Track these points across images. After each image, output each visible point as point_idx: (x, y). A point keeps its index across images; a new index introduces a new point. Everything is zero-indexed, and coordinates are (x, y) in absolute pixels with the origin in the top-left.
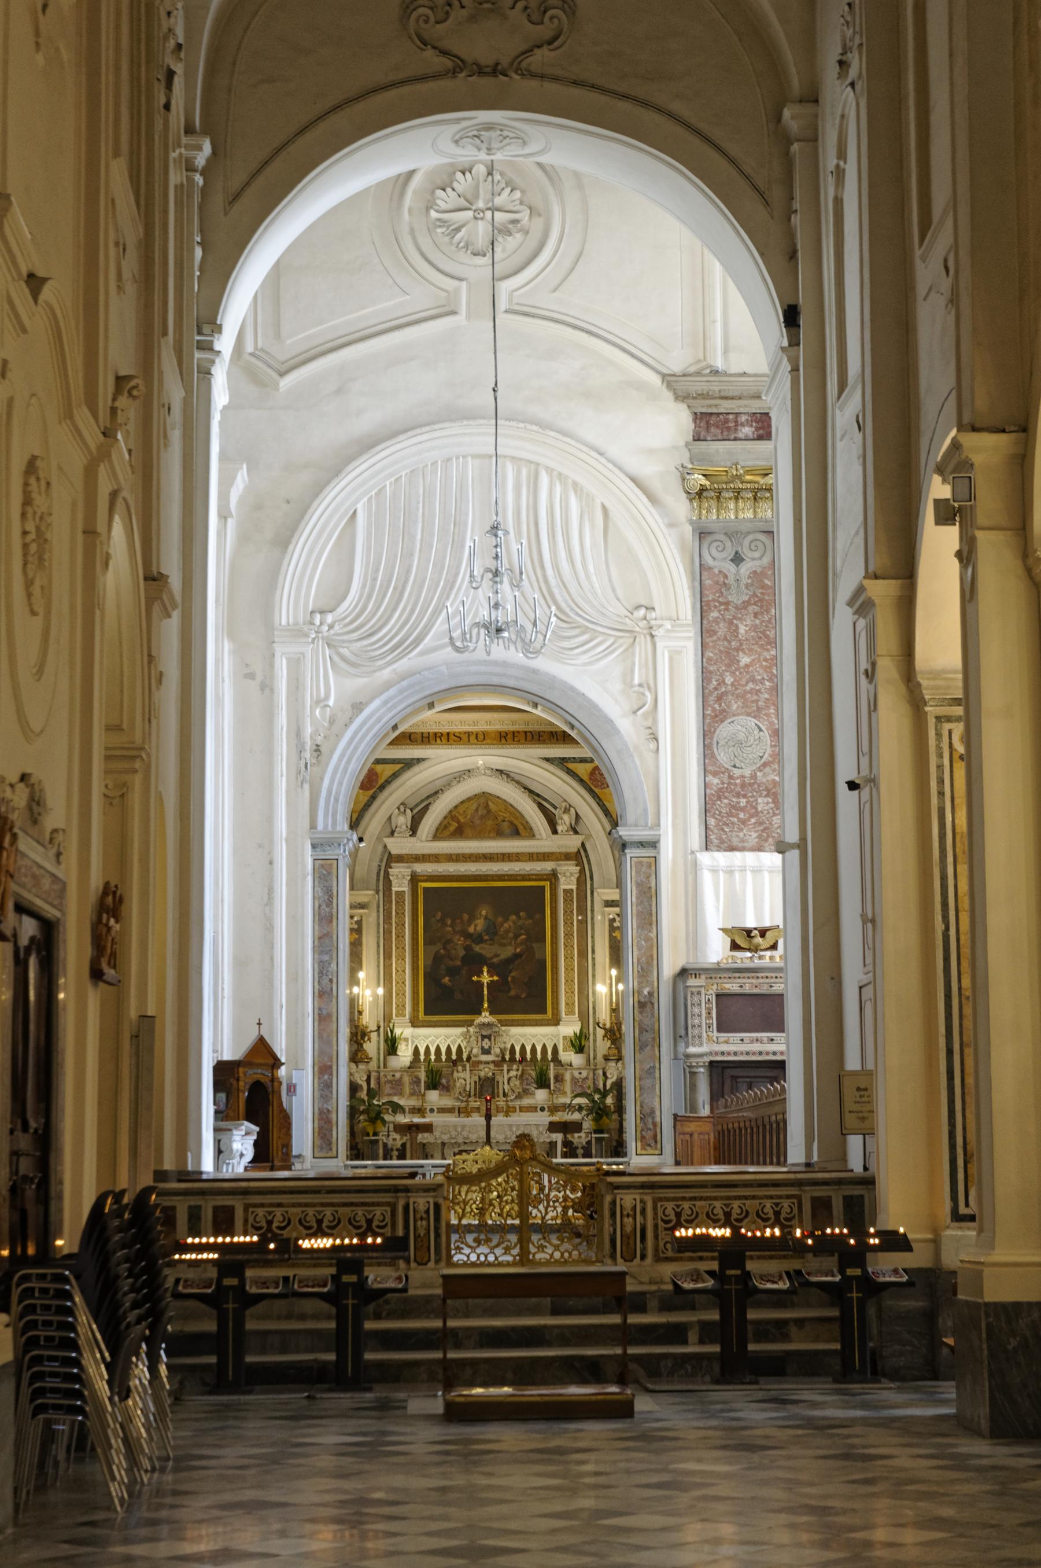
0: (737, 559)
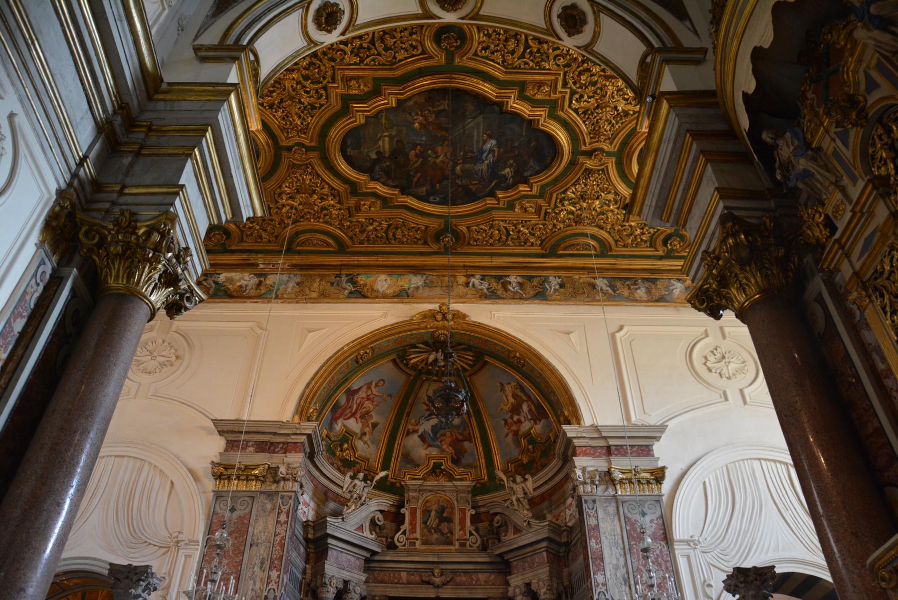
0: (233, 510)
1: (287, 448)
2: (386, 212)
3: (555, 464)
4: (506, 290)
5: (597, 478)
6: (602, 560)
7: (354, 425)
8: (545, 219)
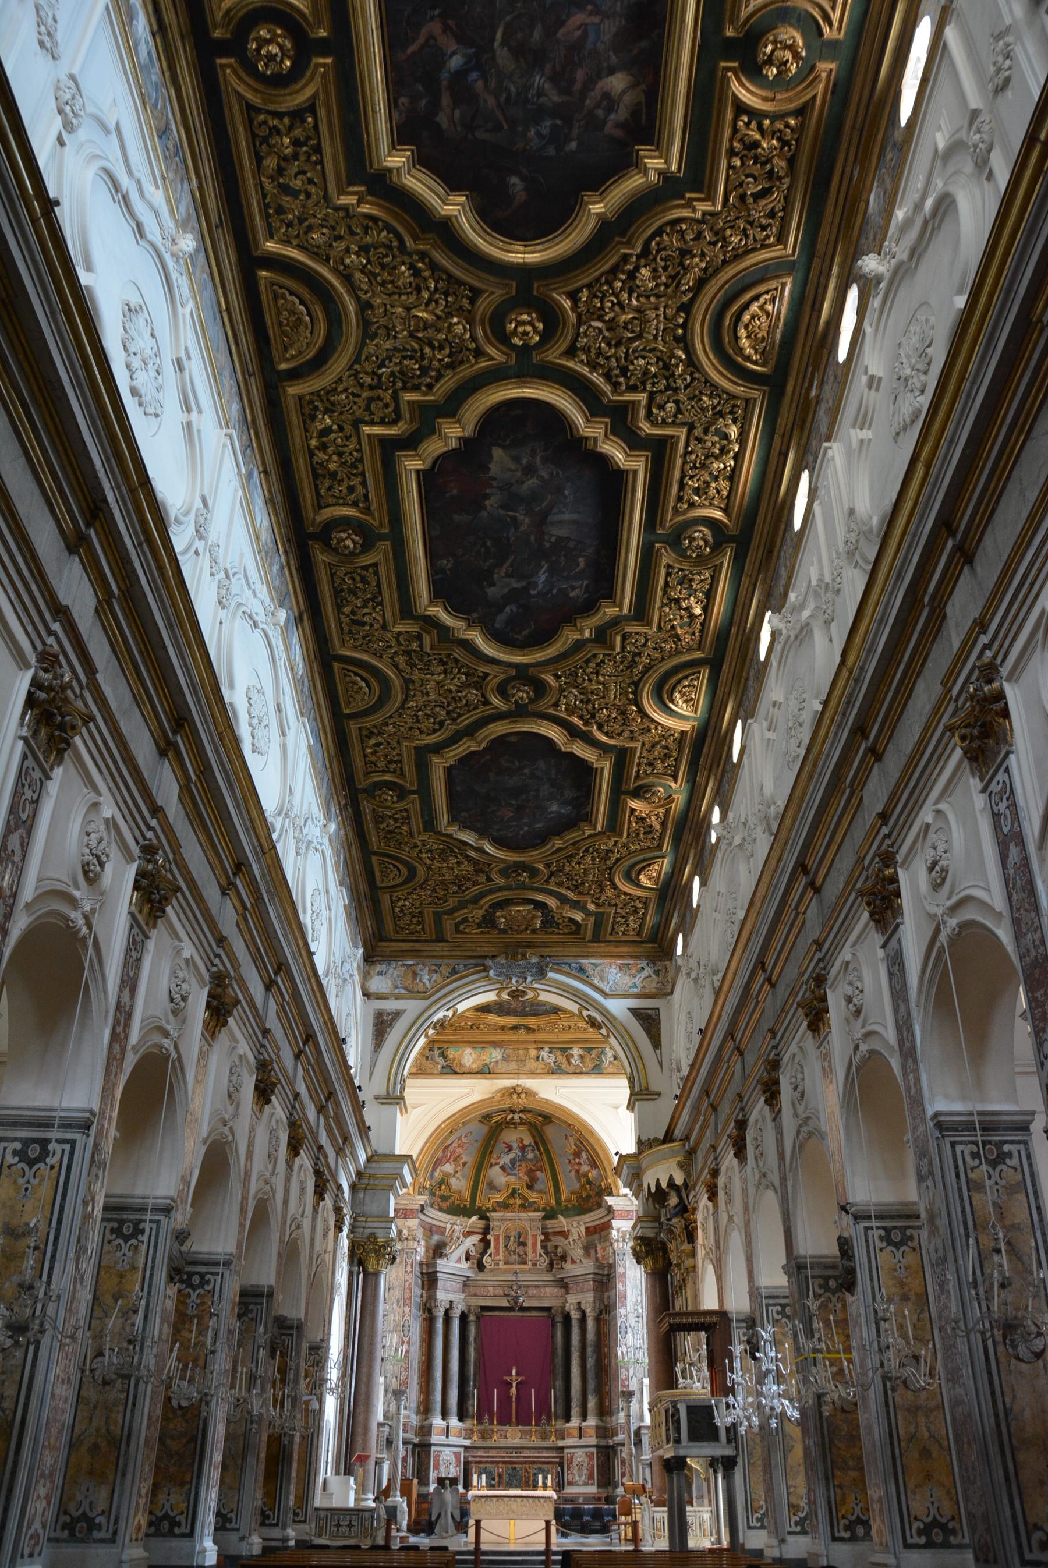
3: (602, 1212)
4: (569, 1063)
7: (448, 1168)
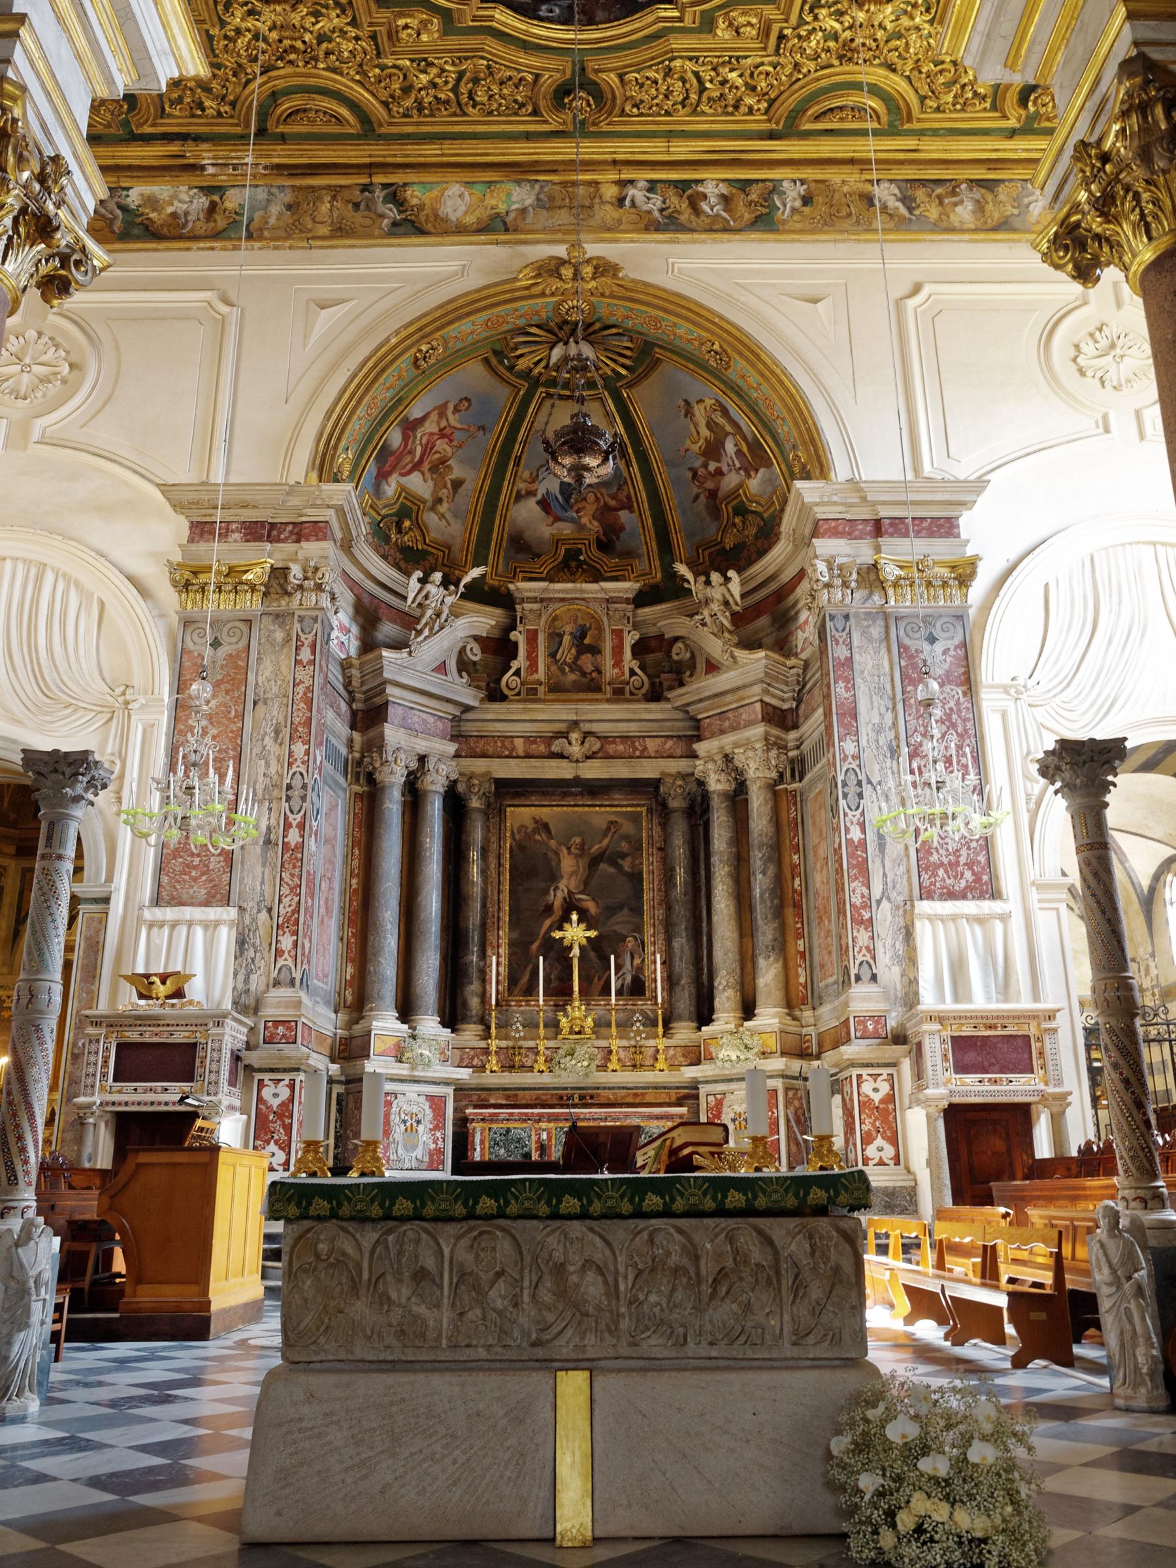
0: (216, 644)
1: (302, 531)
2: (453, 42)
5: (855, 576)
6: (855, 716)
7: (419, 484)
8: (777, 52)
